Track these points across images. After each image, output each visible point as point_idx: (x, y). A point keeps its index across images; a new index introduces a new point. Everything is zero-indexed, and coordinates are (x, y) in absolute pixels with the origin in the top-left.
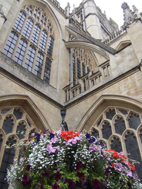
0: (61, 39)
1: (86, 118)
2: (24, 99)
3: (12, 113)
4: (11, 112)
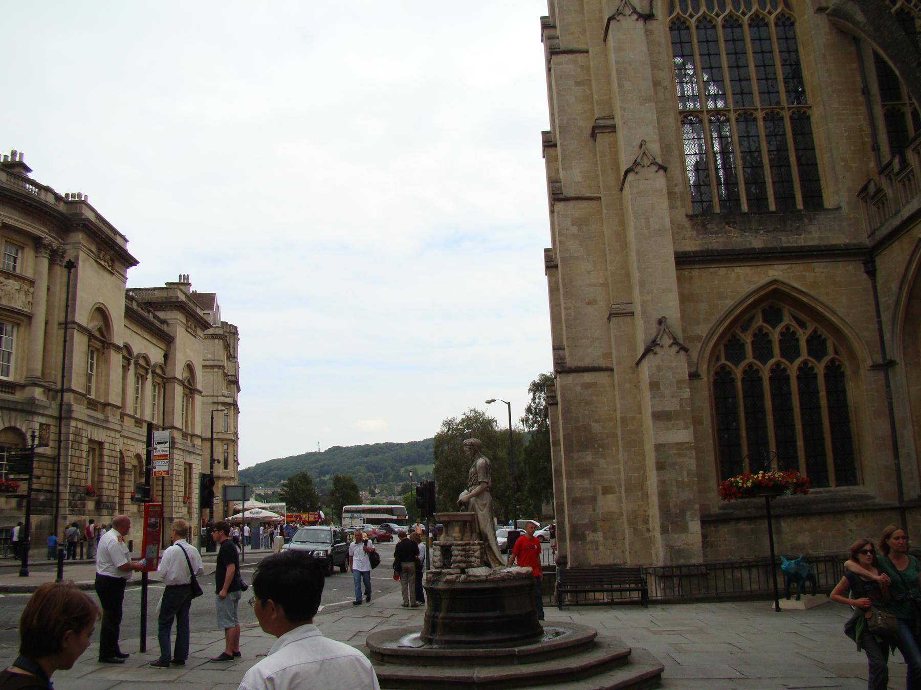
0: (812, 11)
1: (906, 287)
2: (771, 288)
3: (760, 323)
4: (759, 322)
